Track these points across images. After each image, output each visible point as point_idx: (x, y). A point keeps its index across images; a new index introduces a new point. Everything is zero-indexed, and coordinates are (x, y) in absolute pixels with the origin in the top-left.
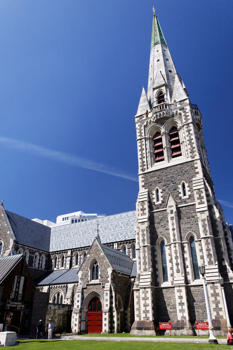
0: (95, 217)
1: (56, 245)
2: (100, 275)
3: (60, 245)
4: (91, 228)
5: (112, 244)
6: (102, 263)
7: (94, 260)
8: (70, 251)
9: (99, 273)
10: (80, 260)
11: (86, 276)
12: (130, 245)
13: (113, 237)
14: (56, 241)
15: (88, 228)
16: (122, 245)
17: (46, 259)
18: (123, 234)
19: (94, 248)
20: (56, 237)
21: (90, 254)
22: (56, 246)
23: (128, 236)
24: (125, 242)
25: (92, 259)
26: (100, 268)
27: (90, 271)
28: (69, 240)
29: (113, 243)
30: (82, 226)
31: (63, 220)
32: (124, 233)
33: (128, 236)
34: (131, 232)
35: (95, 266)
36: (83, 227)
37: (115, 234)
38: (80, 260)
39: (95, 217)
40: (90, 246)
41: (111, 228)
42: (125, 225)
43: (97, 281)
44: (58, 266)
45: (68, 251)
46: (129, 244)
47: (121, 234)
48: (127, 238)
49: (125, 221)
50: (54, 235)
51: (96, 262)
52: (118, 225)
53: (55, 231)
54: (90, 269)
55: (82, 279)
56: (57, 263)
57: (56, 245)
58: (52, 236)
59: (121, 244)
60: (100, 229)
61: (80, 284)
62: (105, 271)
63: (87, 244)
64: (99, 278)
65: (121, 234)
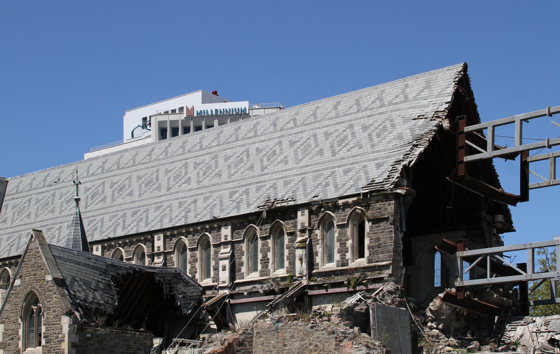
0: (242, 115)
1: (9, 238)
2: (44, 334)
3: (20, 239)
5: (149, 237)
6: (48, 302)
7: (32, 293)
11: (12, 339)
12: (197, 237)
13: (159, 212)
14: (15, 224)
16: (174, 240)
19: (30, 261)
20: (14, 213)
21: (21, 277)
22: (10, 241)
24: (184, 231)
25: (26, 292)
26: (43, 315)
27: (22, 323)
29: (152, 233)
35: (35, 310)
37: (166, 205)
39: (242, 115)
40: (19, 257)
46: (195, 237)
48: (192, 220)
50: (11, 203)
51: (36, 302)
53: (17, 193)
54: (21, 318)
57: (9, 238)
58: (7, 206)
59: (173, 236)
60: (82, 196)
62: (55, 324)
64: (43, 342)
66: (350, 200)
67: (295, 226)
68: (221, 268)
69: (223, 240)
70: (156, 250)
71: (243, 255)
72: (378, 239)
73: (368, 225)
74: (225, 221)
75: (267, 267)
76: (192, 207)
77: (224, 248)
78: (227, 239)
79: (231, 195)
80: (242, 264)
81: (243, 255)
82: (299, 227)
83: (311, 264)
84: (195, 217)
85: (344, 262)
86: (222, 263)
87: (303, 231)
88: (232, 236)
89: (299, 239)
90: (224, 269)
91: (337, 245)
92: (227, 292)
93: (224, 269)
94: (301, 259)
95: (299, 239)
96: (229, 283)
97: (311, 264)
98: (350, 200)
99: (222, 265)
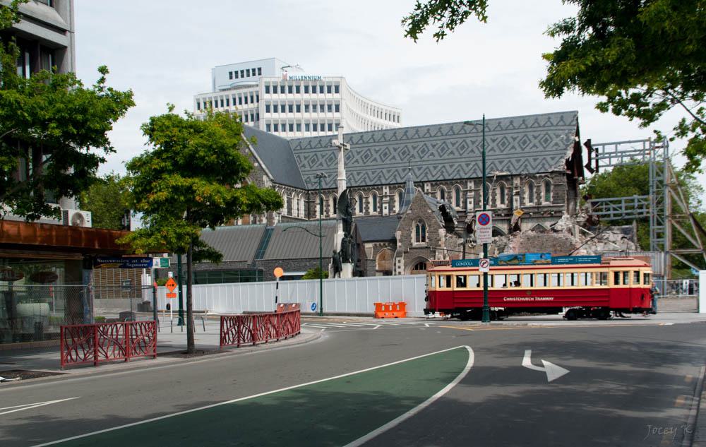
4: (375, 150)
9: (427, 234)
10: (367, 206)
15: (369, 150)
17: (305, 201)
18: (439, 168)
23: (447, 172)
30: (355, 142)
31: (231, 78)
32: (440, 166)
33: (447, 172)
34: (451, 166)
36: (357, 146)
37: (424, 167)
38: (367, 206)
41: (415, 152)
42: (439, 150)
43: (423, 244)
44: (327, 213)
47: (435, 168)
49: (438, 142)
52: (426, 149)
55: (400, 241)
56: (325, 208)
61: (400, 247)
63: (376, 179)
64: (427, 240)
65: (435, 168)
66: (543, 175)
67: (512, 184)
68: (468, 203)
69: (469, 189)
70: (426, 191)
72: (558, 194)
73: (552, 187)
74: (470, 179)
76: (443, 169)
79: (468, 165)
82: (514, 186)
83: (522, 203)
84: (449, 175)
85: (539, 203)
87: (516, 188)
88: (475, 187)
89: (514, 191)
90: (470, 203)
91: (535, 195)
93: (470, 203)
94: (516, 201)
95: (514, 191)
97: (522, 203)
98: (543, 175)
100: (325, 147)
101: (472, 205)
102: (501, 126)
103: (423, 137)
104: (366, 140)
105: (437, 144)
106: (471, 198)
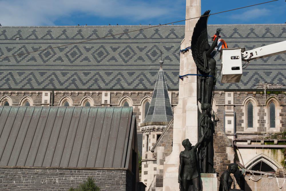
8: (49, 93)
28: (83, 68)
45: (44, 93)
69: (227, 103)
71: (243, 115)
75: (263, 125)
77: (228, 109)
78: (230, 103)
80: (242, 121)
81: (243, 115)
86: (227, 118)
90: (230, 122)
92: (232, 138)
93: (230, 122)
96: (234, 133)
99: (228, 120)
100: (11, 39)
101: (232, 126)
102: (254, 33)
103: (151, 38)
104: (71, 36)
105: (173, 47)
106: (231, 115)
